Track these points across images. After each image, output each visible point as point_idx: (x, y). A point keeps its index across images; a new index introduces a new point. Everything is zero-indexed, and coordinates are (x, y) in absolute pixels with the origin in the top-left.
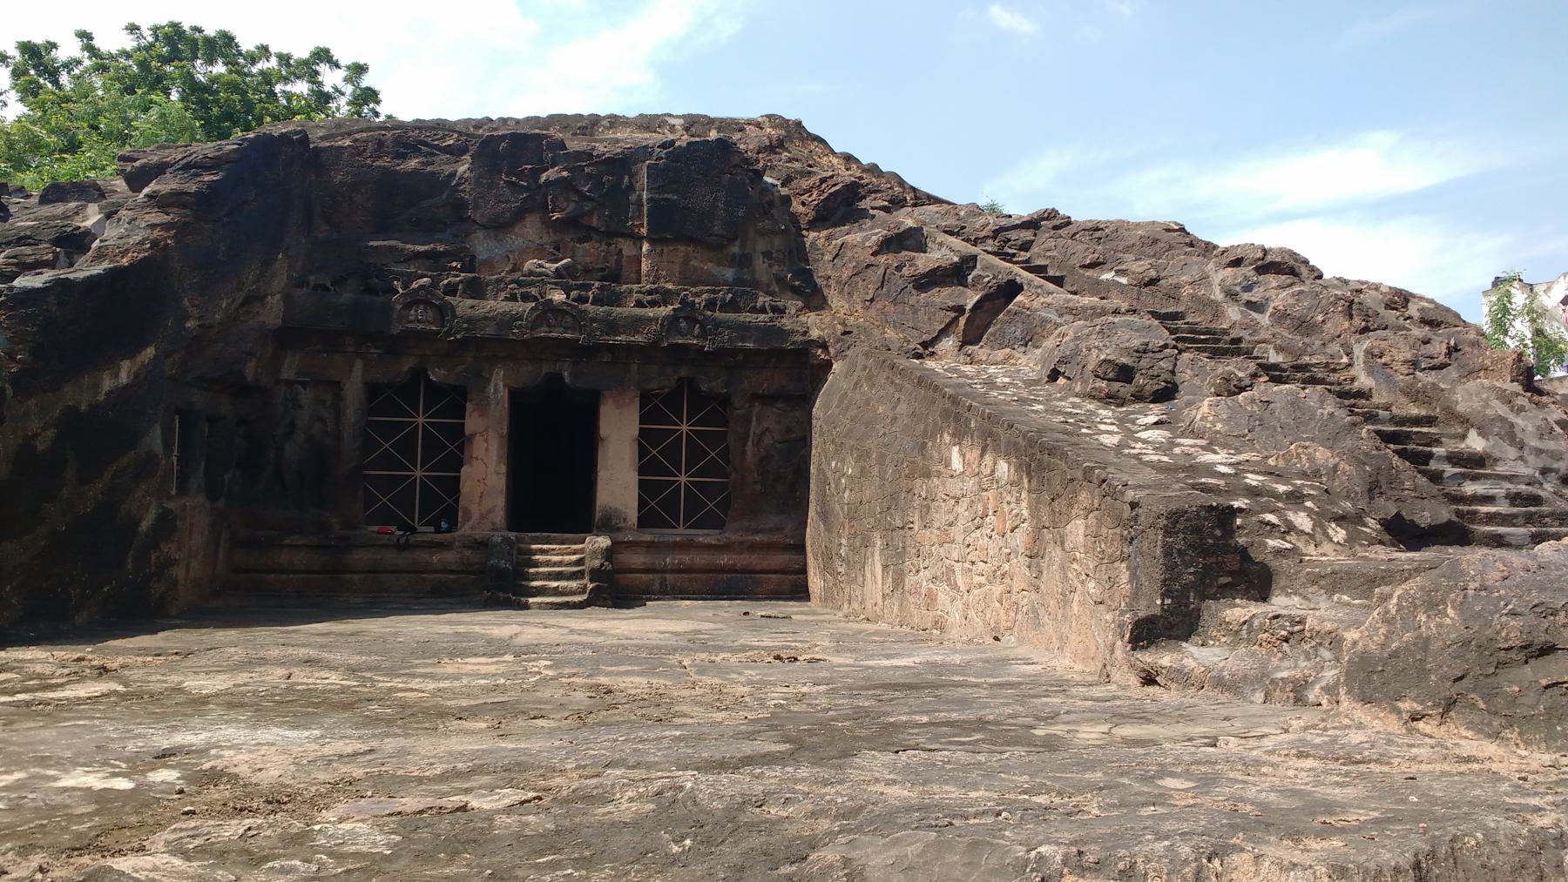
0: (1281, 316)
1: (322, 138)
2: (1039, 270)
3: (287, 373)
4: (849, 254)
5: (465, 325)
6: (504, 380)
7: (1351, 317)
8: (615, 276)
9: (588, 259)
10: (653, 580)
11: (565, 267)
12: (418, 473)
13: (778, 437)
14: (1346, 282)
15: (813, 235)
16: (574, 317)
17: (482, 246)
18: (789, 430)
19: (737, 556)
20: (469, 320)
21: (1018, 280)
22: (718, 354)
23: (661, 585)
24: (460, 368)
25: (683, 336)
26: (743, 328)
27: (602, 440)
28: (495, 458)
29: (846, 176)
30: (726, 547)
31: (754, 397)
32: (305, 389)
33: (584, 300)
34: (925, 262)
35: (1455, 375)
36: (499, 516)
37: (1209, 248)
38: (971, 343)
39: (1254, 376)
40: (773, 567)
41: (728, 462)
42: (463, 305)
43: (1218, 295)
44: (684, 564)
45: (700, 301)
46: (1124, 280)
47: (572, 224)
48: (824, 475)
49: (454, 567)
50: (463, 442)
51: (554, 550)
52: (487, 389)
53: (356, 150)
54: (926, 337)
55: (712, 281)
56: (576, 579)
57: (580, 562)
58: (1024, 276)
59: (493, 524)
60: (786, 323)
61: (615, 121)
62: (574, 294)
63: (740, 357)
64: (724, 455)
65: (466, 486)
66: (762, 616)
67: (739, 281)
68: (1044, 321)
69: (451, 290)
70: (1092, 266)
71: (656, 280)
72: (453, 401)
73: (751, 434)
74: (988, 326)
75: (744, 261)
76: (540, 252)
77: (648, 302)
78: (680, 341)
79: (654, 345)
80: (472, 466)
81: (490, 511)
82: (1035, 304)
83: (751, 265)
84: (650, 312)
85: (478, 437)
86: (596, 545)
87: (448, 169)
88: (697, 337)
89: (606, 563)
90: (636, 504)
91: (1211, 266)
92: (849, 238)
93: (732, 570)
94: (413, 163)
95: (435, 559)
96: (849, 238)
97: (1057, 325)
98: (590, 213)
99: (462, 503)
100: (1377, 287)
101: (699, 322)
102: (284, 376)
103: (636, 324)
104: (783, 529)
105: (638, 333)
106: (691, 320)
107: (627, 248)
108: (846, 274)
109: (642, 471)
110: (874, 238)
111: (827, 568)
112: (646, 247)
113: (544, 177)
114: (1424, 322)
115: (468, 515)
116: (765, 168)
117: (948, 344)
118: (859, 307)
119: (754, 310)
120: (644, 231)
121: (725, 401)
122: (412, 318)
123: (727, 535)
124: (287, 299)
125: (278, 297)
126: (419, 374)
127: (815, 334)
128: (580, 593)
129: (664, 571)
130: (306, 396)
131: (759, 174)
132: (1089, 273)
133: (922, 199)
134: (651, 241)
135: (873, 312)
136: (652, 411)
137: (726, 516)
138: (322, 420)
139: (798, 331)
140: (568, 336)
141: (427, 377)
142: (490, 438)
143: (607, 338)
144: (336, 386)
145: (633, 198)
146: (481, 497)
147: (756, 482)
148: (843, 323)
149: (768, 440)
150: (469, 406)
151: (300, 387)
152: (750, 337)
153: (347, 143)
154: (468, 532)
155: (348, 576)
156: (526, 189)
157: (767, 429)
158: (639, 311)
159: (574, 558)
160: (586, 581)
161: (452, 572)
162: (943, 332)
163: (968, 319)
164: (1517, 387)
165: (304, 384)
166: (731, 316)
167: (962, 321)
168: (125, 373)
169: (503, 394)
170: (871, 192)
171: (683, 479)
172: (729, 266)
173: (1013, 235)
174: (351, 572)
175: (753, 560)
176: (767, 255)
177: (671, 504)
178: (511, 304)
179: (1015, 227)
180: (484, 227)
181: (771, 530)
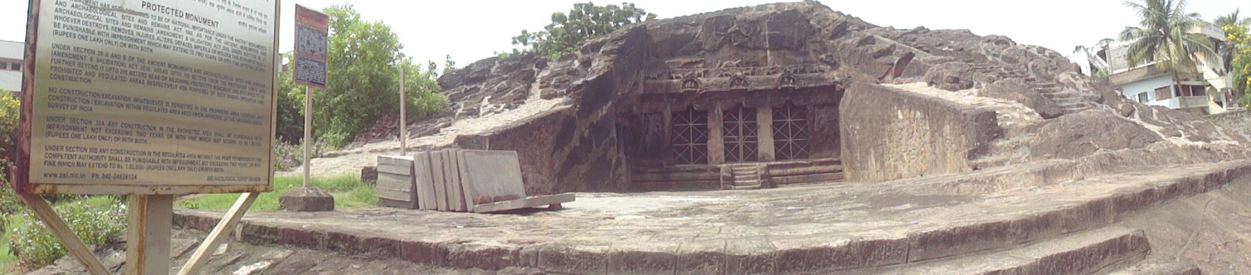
0: (1004, 58)
1: (651, 26)
2: (920, 48)
4: (847, 48)
7: (1026, 57)
8: (756, 64)
9: (747, 59)
11: (740, 63)
13: (827, 120)
14: (1024, 46)
15: (832, 41)
17: (709, 59)
21: (913, 52)
22: (802, 89)
26: (810, 79)
29: (842, 19)
30: (811, 164)
31: (815, 106)
33: (748, 74)
34: (876, 48)
35: (1059, 71)
36: (723, 158)
37: (979, 37)
38: (897, 76)
39: (998, 77)
41: (807, 131)
42: (703, 80)
43: (984, 52)
45: (792, 72)
46: (951, 50)
47: (741, 46)
48: (847, 131)
53: (661, 29)
54: (881, 76)
55: (796, 63)
57: (756, 173)
58: (914, 50)
60: (826, 75)
61: (748, 8)
62: (744, 72)
64: (806, 129)
65: (710, 148)
67: (804, 62)
68: (925, 66)
69: (700, 75)
70: (939, 45)
71: (774, 64)
72: (702, 116)
74: (903, 70)
75: (806, 54)
76: (730, 58)
82: (921, 60)
84: (773, 76)
87: (694, 31)
90: (774, 150)
91: (981, 43)
92: (846, 41)
94: (682, 31)
95: (701, 175)
96: (846, 41)
97: (929, 67)
99: (709, 154)
100: (1034, 46)
101: (791, 78)
102: (644, 112)
103: (768, 81)
105: (768, 85)
106: (789, 78)
107: (761, 54)
108: (846, 55)
109: (774, 139)
110: (856, 41)
111: (852, 167)
112: (768, 52)
113: (729, 31)
114: (1050, 57)
115: (711, 157)
116: (811, 18)
117: (889, 77)
118: (853, 67)
119: (812, 72)
120: (767, 46)
121: (804, 108)
124: (645, 84)
126: (690, 107)
127: (837, 79)
130: (651, 118)
131: (809, 21)
132: (939, 48)
133: (870, 26)
134: (771, 50)
135: (858, 69)
136: (778, 114)
141: (693, 109)
144: (661, 114)
145: (762, 33)
148: (848, 74)
149: (822, 122)
150: (709, 118)
151: (649, 116)
153: (659, 27)
156: (724, 35)
158: (770, 76)
159: (754, 172)
160: (759, 179)
162: (887, 73)
163: (896, 68)
164: (1076, 73)
165: (650, 114)
166: (803, 75)
167: (893, 69)
168: (604, 110)
170: (851, 25)
173: (909, 36)
174: (673, 181)
175: (822, 168)
176: (815, 51)
177: (787, 150)
178: (721, 78)
179: (909, 33)
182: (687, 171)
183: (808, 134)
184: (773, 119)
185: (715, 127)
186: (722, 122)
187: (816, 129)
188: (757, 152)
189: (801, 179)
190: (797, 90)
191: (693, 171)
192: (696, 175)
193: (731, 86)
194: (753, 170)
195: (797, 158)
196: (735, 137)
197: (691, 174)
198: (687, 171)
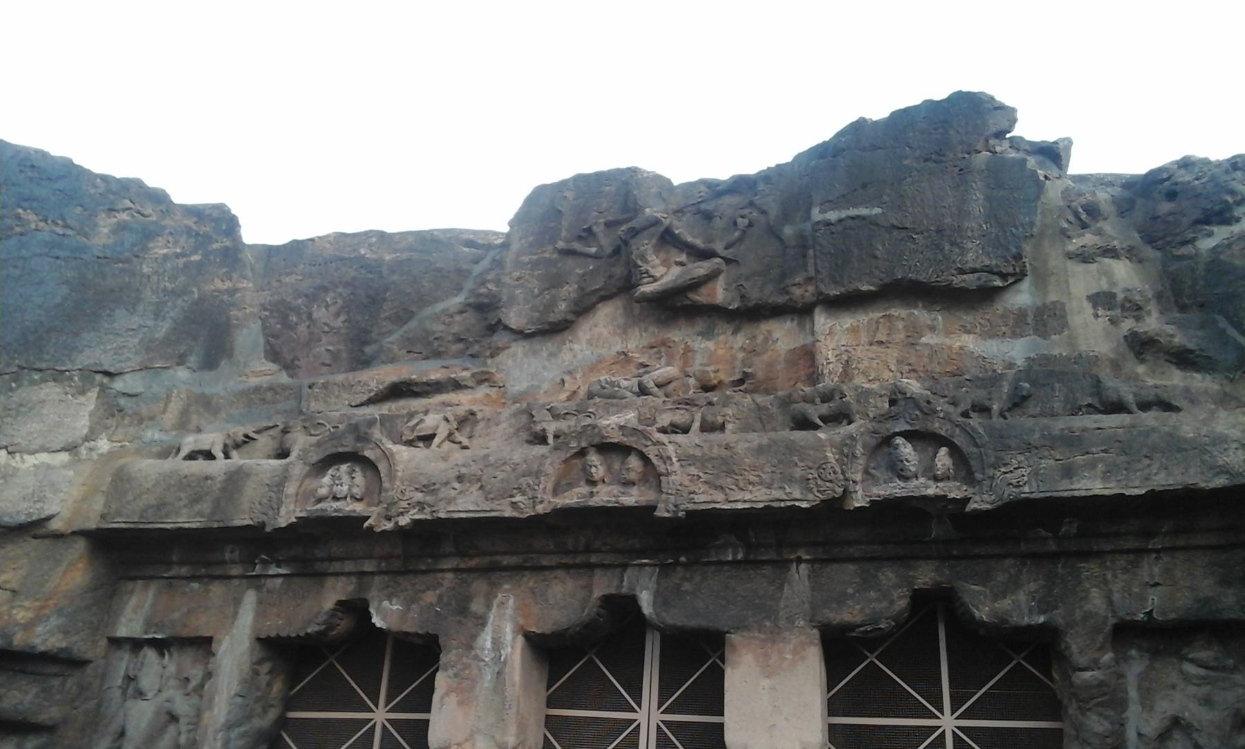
3: (129, 625)
5: (419, 496)
20: (427, 488)
24: (430, 597)
52: (479, 641)
77: (822, 418)
83: (1065, 325)
98: (712, 277)
102: (122, 632)
150: (441, 681)
152: (1092, 465)
158: (800, 436)
165: (160, 646)
169: (514, 650)
172: (1015, 335)
176: (1102, 300)
180: (521, 335)
184: (833, 707)
190: (978, 514)
193: (555, 492)
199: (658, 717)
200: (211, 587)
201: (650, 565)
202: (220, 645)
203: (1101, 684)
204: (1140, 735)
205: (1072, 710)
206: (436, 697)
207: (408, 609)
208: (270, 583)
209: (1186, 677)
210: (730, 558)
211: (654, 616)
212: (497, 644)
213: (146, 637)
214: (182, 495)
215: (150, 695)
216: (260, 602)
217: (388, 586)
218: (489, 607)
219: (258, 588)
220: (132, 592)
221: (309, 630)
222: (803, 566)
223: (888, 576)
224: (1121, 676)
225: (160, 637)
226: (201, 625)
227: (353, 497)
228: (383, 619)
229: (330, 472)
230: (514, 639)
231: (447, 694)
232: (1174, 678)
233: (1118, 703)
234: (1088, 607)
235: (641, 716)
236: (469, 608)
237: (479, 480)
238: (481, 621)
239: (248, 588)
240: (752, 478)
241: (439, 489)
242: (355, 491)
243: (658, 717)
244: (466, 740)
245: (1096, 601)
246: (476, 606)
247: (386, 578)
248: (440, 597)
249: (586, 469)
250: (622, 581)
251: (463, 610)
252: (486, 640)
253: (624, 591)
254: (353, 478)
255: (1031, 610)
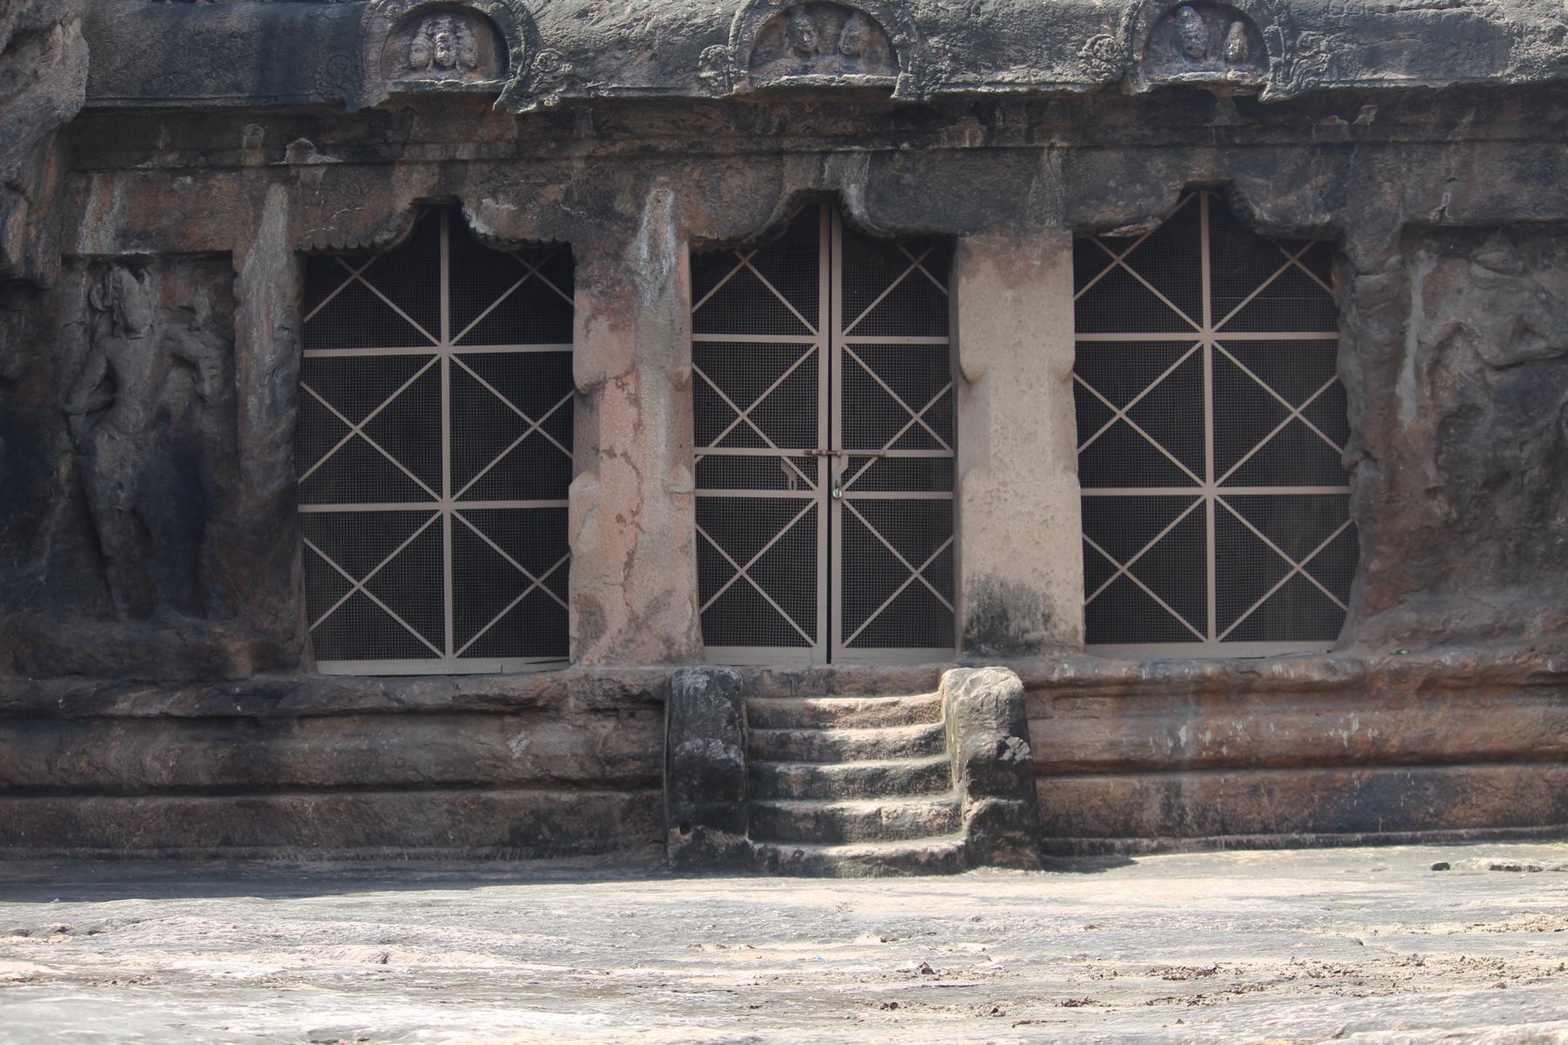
3: (95, 238)
5: (566, 68)
6: (675, 218)
10: (1144, 792)
12: (447, 505)
13: (1491, 351)
16: (871, 21)
18: (1525, 330)
19: (1388, 716)
20: (577, 53)
23: (1167, 808)
24: (554, 192)
25: (1195, 59)
27: (969, 383)
28: (662, 449)
30: (1355, 689)
31: (1414, 234)
32: (139, 278)
40: (1495, 745)
41: (1342, 432)
44: (1230, 743)
49: (572, 770)
50: (568, 409)
51: (850, 710)
52: (631, 249)
56: (926, 790)
57: (930, 743)
59: (669, 642)
63: (1368, 115)
64: (1334, 411)
65: (584, 536)
66: (1494, 868)
73: (1411, 345)
78: (1187, 76)
79: (1111, 92)
80: (597, 474)
81: (656, 606)
85: (611, 386)
86: (979, 691)
88: (1238, 61)
89: (1014, 741)
93: (1376, 758)
95: (517, 745)
101: (1235, 15)
102: (86, 247)
104: (1521, 628)
105: (1060, 56)
109: (1091, 469)
115: (595, 618)
122: (419, 57)
123: (1351, 653)
125: (77, 24)
128: (941, 830)
129: (1174, 767)
137: (1346, 601)
138: (188, 364)
139: (1536, 30)
140: (858, 78)
142: (644, 394)
143: (971, 76)
146: (629, 565)
147: (1431, 493)
149: (1460, 362)
150: (582, 302)
151: (126, 275)
152: (1397, 53)
154: (600, 669)
155: (285, 800)
157: (1458, 329)
161: (563, 783)
165: (135, 266)
169: (676, 260)
171: (1210, 491)
181: (1486, 634)
182: (414, 713)
183: (1347, 455)
185: (633, 369)
186: (687, 337)
187: (1408, 414)
188: (946, 573)
189: (1269, 807)
190: (1274, 106)
191: (456, 713)
192: (482, 740)
194: (911, 718)
195: (1252, 631)
196: (785, 453)
197: (429, 732)
198: (414, 713)
199: (841, 340)
200: (212, 182)
201: (859, 152)
202: (243, 261)
203: (1385, 289)
204: (1420, 343)
205: (1352, 316)
206: (578, 322)
207: (523, 209)
208: (303, 173)
209: (1474, 281)
210: (967, 145)
211: (866, 217)
212: (655, 254)
213: (125, 253)
214: (201, 62)
215: (144, 331)
216: (293, 202)
217: (489, 179)
218: (640, 206)
219: (289, 182)
220: (87, 190)
221: (378, 239)
222: (1055, 153)
223: (1157, 165)
224: (1405, 280)
225: (147, 252)
226: (211, 233)
227: (464, 64)
228: (488, 223)
229: (423, 29)
230: (678, 245)
231: (593, 317)
232: (1461, 281)
233: (1400, 309)
234: (1379, 204)
235: (819, 340)
236: (612, 207)
237: (650, 47)
238: (629, 224)
239: (270, 182)
240: (1012, 53)
241: (594, 58)
242: (467, 56)
243: (841, 340)
244: (627, 373)
245: (1387, 196)
246: (622, 205)
247: (485, 168)
248: (568, 193)
249: (794, 34)
250: (822, 173)
251: (604, 210)
252: (639, 249)
253: (827, 184)
254: (459, 38)
255: (1317, 207)
